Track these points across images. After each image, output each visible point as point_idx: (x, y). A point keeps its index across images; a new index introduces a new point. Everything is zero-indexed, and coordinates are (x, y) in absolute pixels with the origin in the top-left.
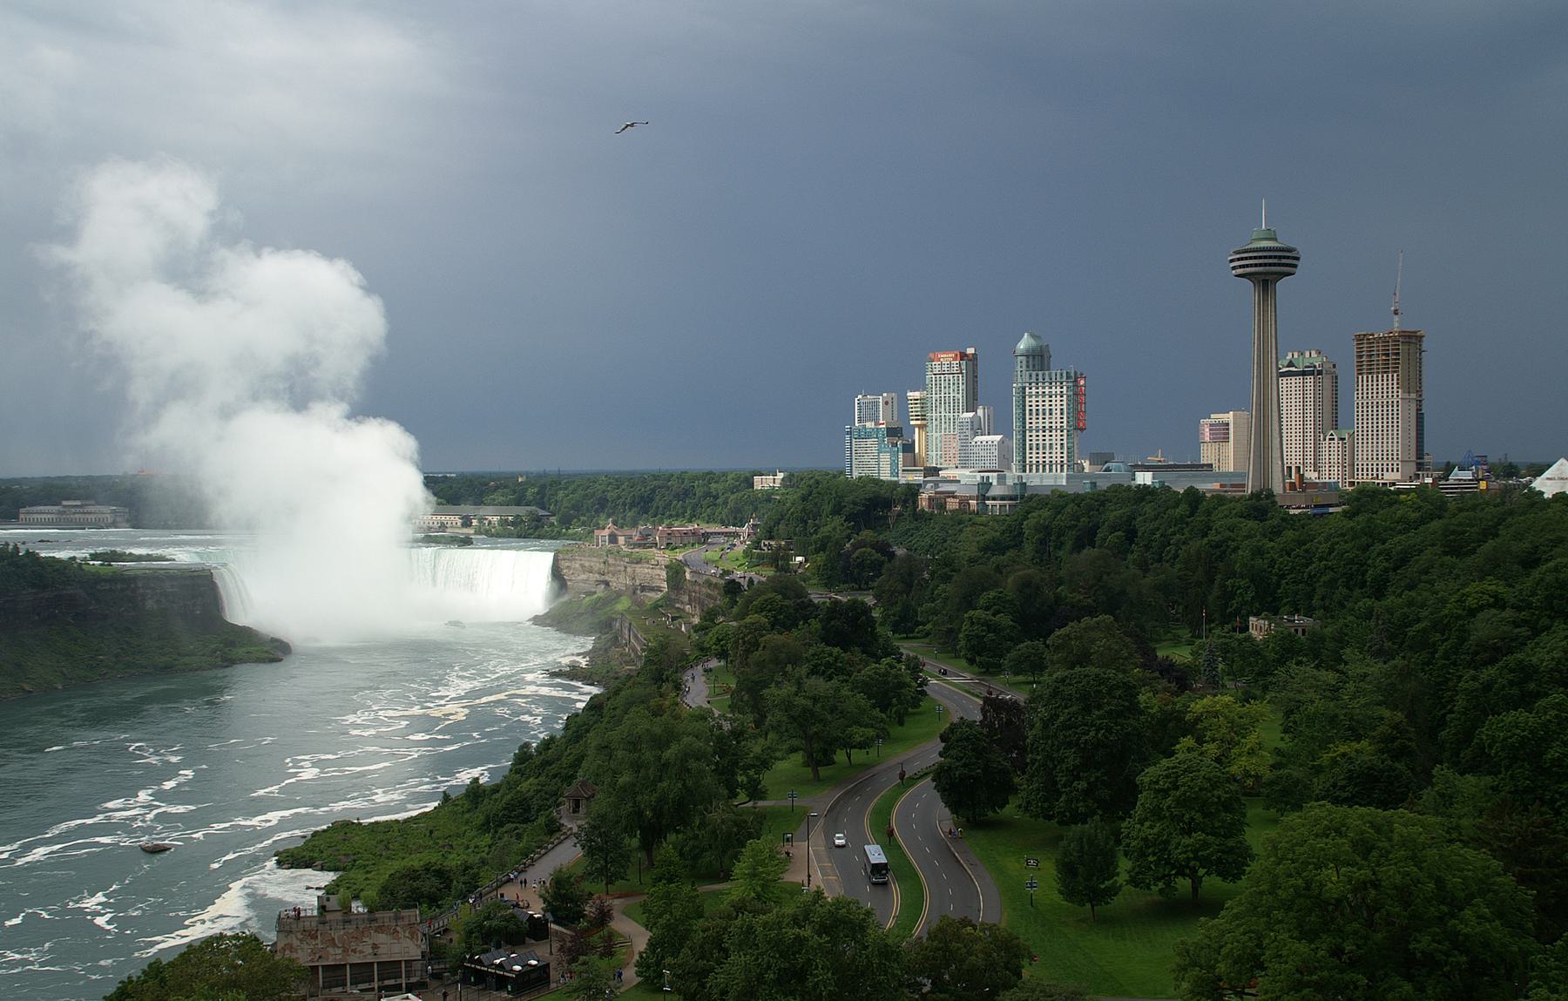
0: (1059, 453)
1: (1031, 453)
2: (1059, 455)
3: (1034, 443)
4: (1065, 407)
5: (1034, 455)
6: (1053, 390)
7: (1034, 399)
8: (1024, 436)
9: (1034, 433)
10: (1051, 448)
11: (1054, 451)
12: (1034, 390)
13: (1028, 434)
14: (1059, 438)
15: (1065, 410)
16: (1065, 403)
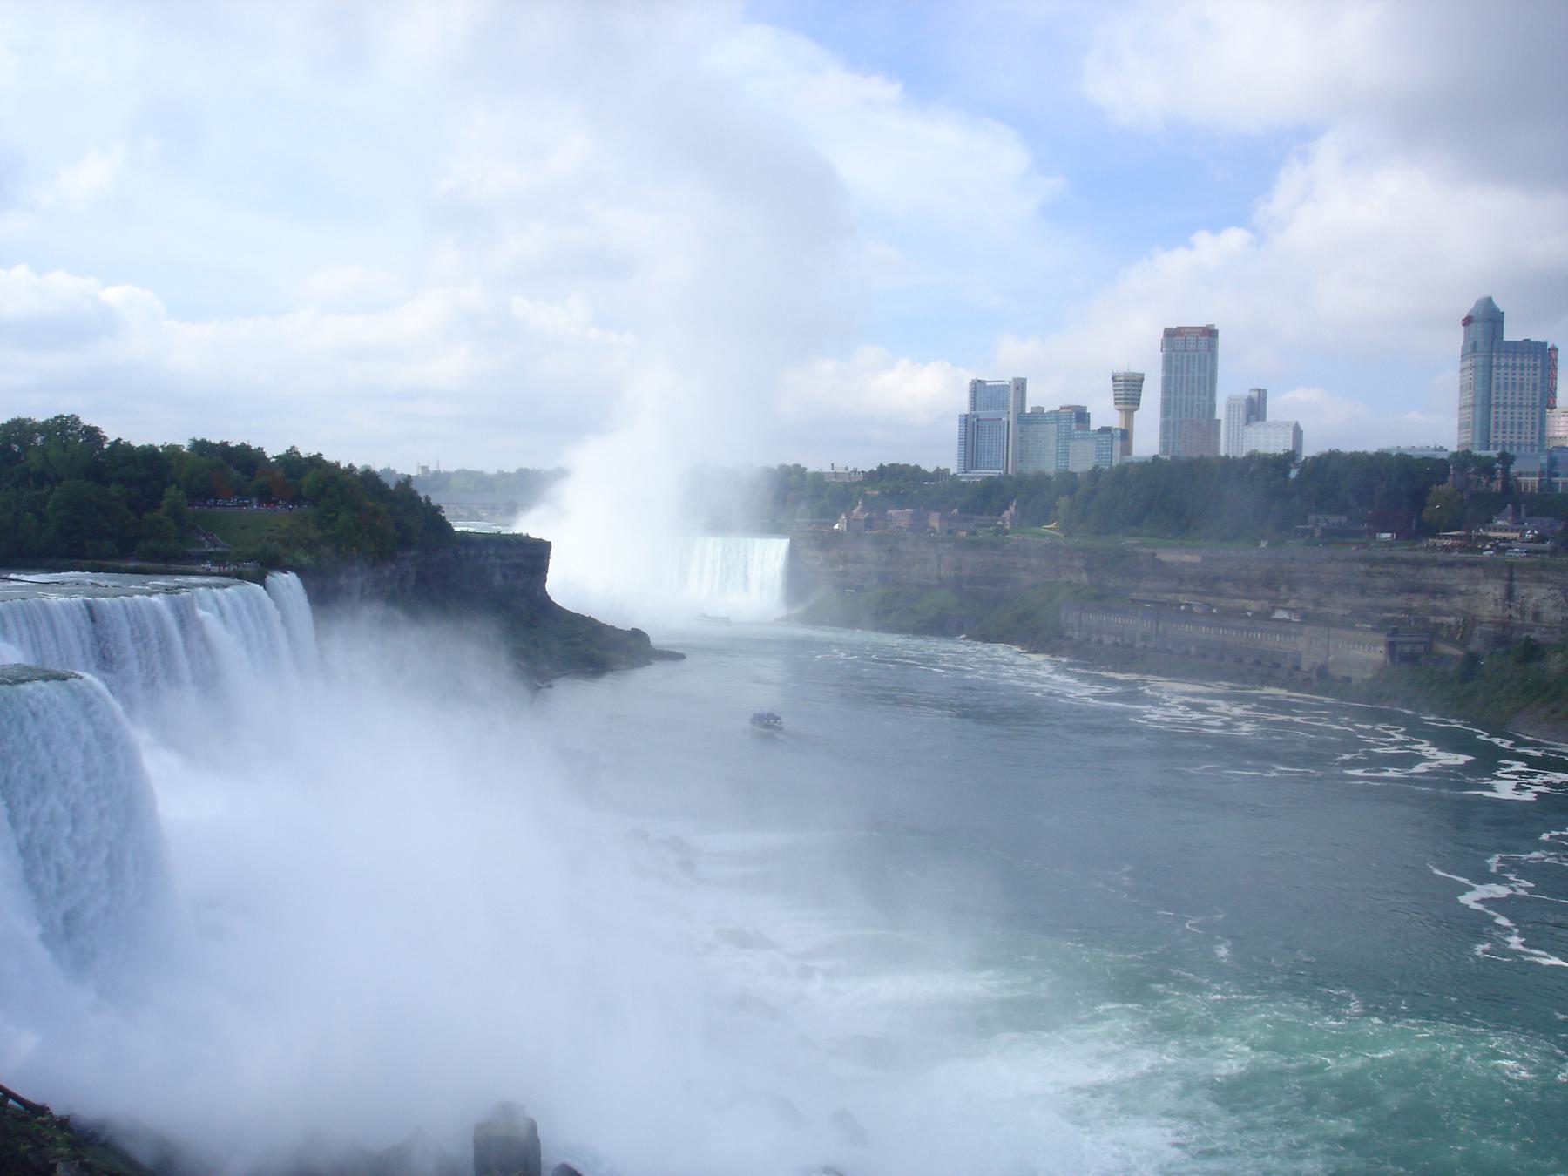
0: (1529, 433)
1: (1496, 432)
2: (1529, 436)
3: (1501, 420)
4: (1538, 381)
5: (1500, 434)
6: (1526, 363)
7: (1502, 371)
8: (1489, 413)
9: (1501, 410)
10: (1520, 427)
11: (1524, 430)
12: (1502, 361)
13: (1493, 410)
14: (1530, 416)
15: (1539, 386)
16: (1538, 377)
